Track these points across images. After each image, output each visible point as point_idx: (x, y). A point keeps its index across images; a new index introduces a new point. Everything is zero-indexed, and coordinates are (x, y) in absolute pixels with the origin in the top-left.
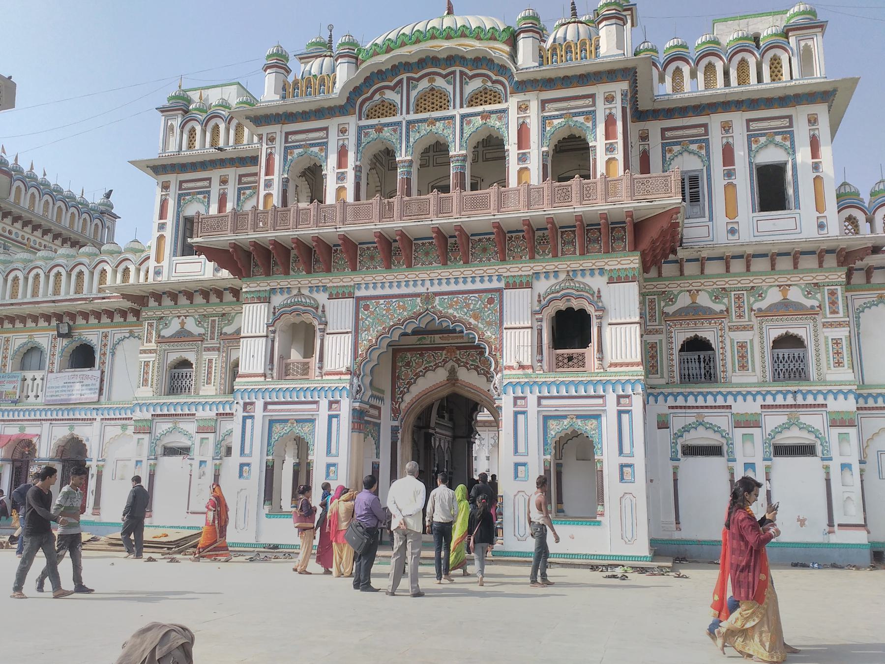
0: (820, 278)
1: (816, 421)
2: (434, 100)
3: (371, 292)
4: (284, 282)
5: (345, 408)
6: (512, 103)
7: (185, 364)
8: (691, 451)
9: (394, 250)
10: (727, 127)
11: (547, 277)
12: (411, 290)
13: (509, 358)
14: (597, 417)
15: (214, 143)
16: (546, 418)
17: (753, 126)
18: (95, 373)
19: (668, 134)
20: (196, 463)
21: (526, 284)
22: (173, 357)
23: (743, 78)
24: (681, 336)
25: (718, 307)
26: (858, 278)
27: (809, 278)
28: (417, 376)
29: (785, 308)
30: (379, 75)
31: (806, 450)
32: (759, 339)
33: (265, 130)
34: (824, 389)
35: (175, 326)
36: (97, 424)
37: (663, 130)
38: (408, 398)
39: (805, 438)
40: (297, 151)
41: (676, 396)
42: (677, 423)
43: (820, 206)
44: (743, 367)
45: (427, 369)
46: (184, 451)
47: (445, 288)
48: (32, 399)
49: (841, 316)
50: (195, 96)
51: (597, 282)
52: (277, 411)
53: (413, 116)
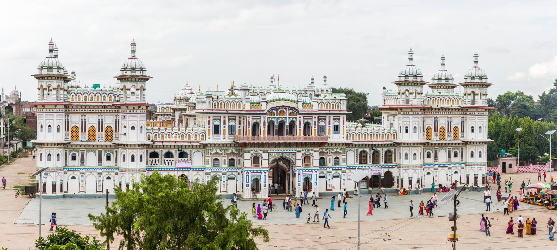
1: (340, 172)
5: (267, 173)
6: (298, 116)
10: (329, 117)
13: (297, 165)
15: (221, 108)
20: (222, 182)
22: (214, 158)
23: (333, 108)
30: (273, 108)
31: (338, 177)
32: (332, 158)
35: (214, 151)
36: (191, 172)
43: (343, 134)
50: (213, 93)
51: (312, 152)
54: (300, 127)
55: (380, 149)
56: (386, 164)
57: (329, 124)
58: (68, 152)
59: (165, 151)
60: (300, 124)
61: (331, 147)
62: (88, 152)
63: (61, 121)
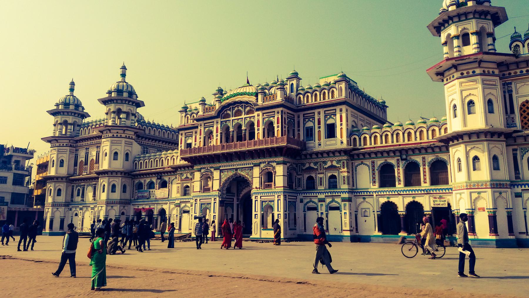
0: (340, 158)
1: (339, 200)
2: (238, 113)
3: (223, 168)
4: (204, 166)
6: (256, 114)
7: (188, 187)
8: (310, 209)
9: (228, 157)
10: (319, 113)
11: (263, 163)
12: (233, 167)
13: (254, 187)
14: (273, 201)
16: (262, 202)
17: (326, 112)
18: (166, 190)
19: (305, 116)
21: (258, 165)
22: (185, 185)
24: (306, 176)
25: (316, 167)
26: (356, 157)
27: (337, 158)
28: (243, 189)
29: (332, 167)
31: (337, 208)
33: (199, 123)
34: (340, 191)
35: (185, 176)
36: (168, 204)
37: (304, 115)
38: (241, 195)
39: (337, 205)
40: (207, 128)
41: (304, 193)
42: (305, 201)
44: (321, 185)
45: (246, 187)
46: (188, 212)
47: (240, 167)
48: (152, 198)
49: (345, 169)
51: (274, 164)
52: (203, 201)
53: (234, 118)
54: (258, 130)
55: (418, 159)
56: (433, 187)
57: (319, 123)
58: (75, 187)
59: (148, 180)
60: (258, 126)
61: (322, 160)
62: (88, 186)
63: (65, 155)
